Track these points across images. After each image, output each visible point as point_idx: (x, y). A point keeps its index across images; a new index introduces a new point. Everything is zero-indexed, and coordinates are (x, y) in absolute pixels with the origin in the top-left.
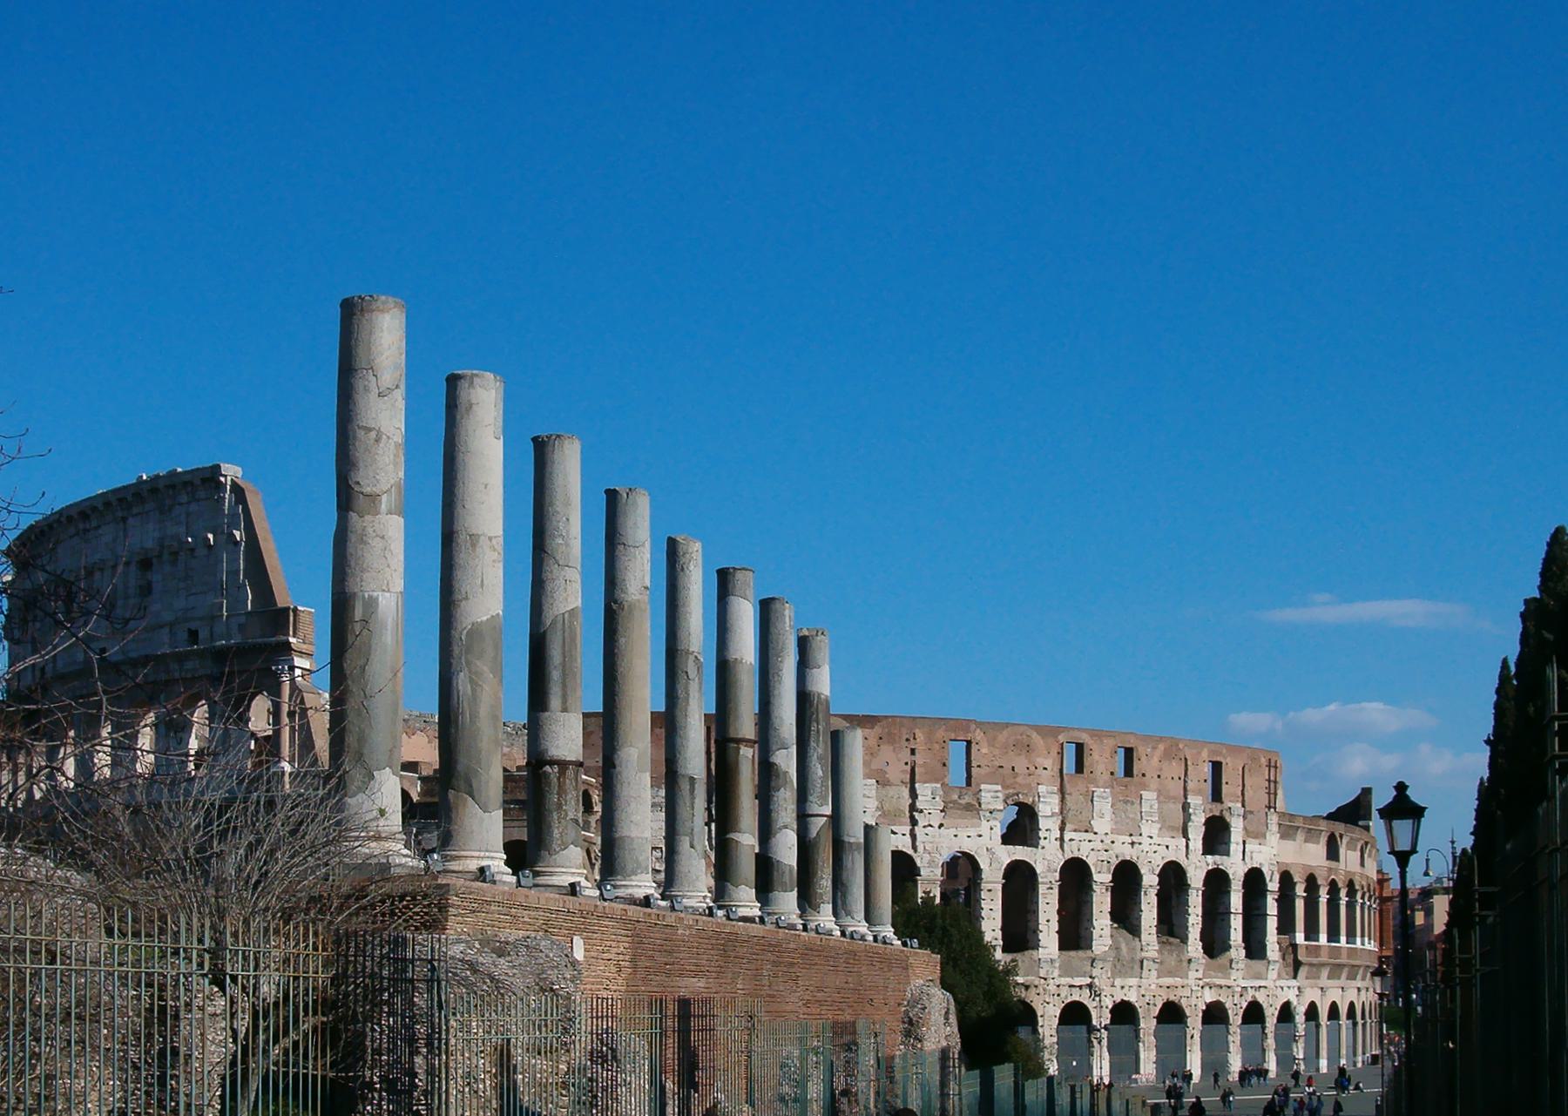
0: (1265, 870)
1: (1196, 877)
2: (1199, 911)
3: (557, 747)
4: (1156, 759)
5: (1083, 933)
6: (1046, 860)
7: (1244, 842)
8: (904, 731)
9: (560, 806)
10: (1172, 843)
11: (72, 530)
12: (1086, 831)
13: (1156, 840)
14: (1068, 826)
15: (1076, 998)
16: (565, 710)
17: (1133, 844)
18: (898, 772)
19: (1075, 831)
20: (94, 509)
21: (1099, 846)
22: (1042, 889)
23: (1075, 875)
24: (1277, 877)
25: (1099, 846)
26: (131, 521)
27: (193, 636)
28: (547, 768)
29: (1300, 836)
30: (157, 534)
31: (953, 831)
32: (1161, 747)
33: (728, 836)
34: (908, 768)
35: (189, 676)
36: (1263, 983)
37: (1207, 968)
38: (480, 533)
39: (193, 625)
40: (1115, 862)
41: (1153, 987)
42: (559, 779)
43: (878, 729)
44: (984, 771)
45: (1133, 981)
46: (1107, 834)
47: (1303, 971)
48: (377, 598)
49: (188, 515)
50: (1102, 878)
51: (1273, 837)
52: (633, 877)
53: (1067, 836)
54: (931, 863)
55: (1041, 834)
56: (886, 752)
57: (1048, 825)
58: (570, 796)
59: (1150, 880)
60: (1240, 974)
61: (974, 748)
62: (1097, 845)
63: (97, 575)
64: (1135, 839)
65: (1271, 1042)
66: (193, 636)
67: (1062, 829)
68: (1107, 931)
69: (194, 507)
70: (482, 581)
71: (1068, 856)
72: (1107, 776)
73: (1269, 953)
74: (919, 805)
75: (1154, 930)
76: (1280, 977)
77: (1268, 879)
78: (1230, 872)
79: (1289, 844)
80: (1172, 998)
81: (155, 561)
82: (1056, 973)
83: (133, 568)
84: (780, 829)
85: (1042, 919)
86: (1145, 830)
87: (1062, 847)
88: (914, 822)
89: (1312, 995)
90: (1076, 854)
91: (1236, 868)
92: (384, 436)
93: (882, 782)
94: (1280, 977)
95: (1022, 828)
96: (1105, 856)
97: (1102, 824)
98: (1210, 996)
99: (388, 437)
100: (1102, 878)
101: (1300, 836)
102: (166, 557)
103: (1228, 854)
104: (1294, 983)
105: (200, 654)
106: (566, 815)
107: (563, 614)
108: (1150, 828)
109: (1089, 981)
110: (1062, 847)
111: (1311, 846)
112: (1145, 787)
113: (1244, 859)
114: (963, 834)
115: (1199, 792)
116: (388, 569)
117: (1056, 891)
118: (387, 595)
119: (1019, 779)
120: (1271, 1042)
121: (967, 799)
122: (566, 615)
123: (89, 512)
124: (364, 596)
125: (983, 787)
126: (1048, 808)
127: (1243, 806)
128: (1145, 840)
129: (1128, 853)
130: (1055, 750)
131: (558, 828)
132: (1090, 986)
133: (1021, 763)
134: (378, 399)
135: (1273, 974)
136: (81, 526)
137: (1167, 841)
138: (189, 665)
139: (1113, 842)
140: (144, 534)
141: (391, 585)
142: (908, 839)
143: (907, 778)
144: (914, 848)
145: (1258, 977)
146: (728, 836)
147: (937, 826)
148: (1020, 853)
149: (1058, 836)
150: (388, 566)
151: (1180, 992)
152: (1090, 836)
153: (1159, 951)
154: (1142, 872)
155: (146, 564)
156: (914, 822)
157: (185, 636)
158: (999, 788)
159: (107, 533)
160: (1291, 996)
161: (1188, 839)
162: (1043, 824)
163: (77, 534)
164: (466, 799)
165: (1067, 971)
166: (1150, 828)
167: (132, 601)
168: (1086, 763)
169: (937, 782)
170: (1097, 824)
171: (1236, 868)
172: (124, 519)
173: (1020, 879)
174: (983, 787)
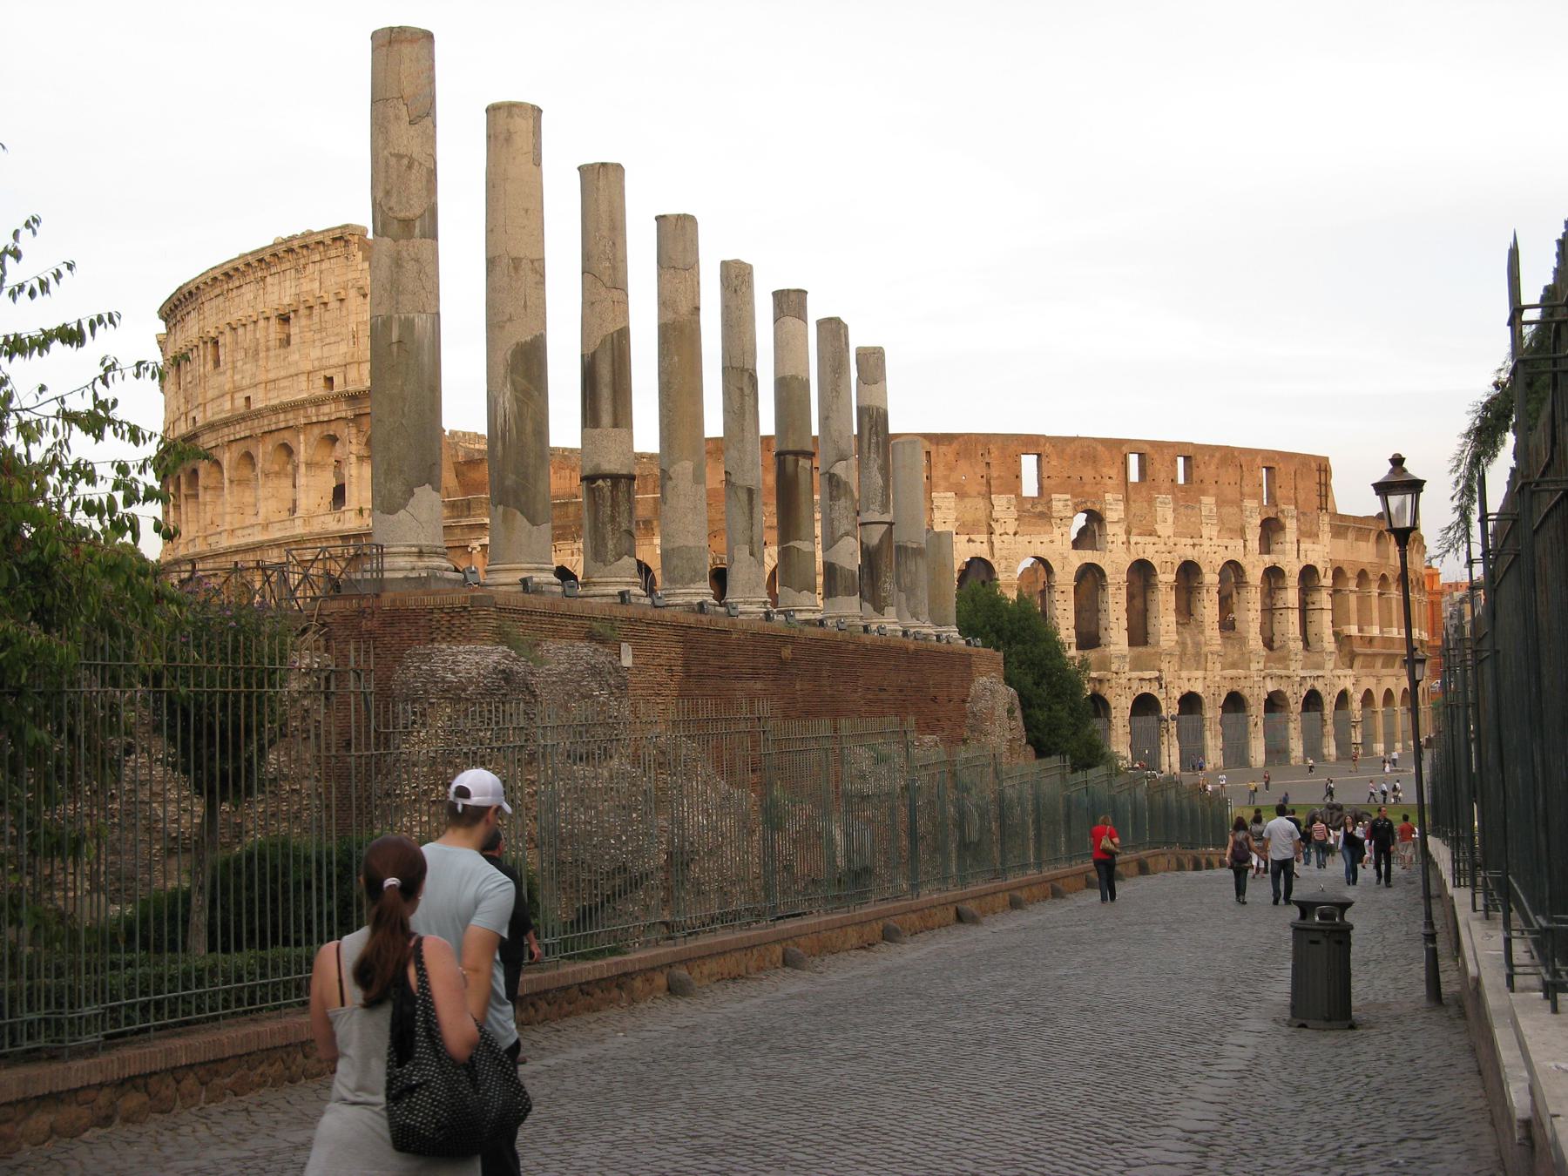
0: (1320, 567)
1: (1254, 575)
2: (1259, 606)
3: (609, 462)
4: (1213, 467)
5: (1151, 629)
6: (1115, 560)
7: (1298, 541)
8: (979, 447)
9: (613, 519)
10: (1231, 544)
11: (218, 291)
12: (1150, 535)
13: (1219, 542)
14: (1134, 531)
15: (1146, 690)
16: (616, 425)
17: (1194, 545)
18: (976, 487)
19: (1140, 535)
20: (237, 269)
21: (1164, 548)
22: (1111, 590)
23: (1142, 572)
24: (1330, 573)
25: (1164, 548)
26: (269, 279)
27: (329, 380)
28: (600, 482)
29: (1351, 535)
30: (293, 290)
31: (1028, 538)
32: (1218, 455)
33: (791, 544)
34: (984, 480)
35: (326, 419)
36: (1320, 673)
37: (1268, 660)
38: (522, 256)
39: (328, 373)
40: (1178, 563)
41: (1217, 679)
42: (612, 492)
43: (955, 445)
44: (1052, 482)
45: (1200, 674)
46: (1169, 537)
47: (1357, 663)
48: (413, 320)
49: (321, 272)
50: (1166, 576)
51: (1325, 536)
52: (692, 586)
53: (1133, 539)
55: (1109, 539)
56: (963, 465)
57: (1114, 532)
58: (622, 508)
59: (1211, 578)
60: (1299, 665)
61: (1043, 458)
62: (1161, 547)
63: (241, 331)
64: (1196, 541)
65: (1329, 728)
66: (329, 380)
67: (1128, 532)
68: (1173, 627)
69: (325, 265)
70: (525, 302)
71: (1135, 557)
72: (1168, 484)
73: (1326, 645)
74: (994, 515)
75: (1216, 626)
76: (1336, 667)
77: (1322, 576)
78: (1286, 570)
79: (1341, 543)
80: (1236, 688)
81: (292, 315)
82: (1127, 668)
83: (273, 321)
84: (842, 536)
85: (1112, 618)
86: (1205, 532)
87: (1128, 549)
89: (1368, 683)
90: (1141, 556)
91: (1292, 568)
92: (416, 164)
93: (961, 494)
94: (1336, 667)
96: (1169, 557)
97: (1165, 528)
98: (1271, 686)
99: (420, 164)
100: (1166, 576)
101: (1351, 535)
102: (302, 311)
103: (1283, 552)
104: (1350, 672)
105: (336, 399)
106: (620, 526)
107: (612, 334)
108: (1209, 531)
109: (1156, 674)
110: (1128, 549)
111: (1362, 544)
112: (1204, 493)
113: (1298, 557)
114: (1036, 540)
115: (1256, 496)
116: (422, 291)
117: (1124, 591)
118: (424, 316)
119: (1087, 488)
120: (1329, 728)
121: (1039, 509)
122: (615, 335)
123: (231, 273)
124: (400, 318)
125: (1053, 496)
126: (1114, 512)
127: (1296, 507)
128: (1206, 542)
129: (1190, 554)
130: (1119, 460)
131: (612, 539)
132: (1159, 679)
133: (1088, 474)
134: (409, 127)
135: (1330, 665)
136: (225, 287)
137: (1226, 542)
138: (325, 409)
139: (1175, 545)
140: (281, 291)
141: (427, 307)
142: (986, 546)
143: (984, 489)
144: (993, 555)
145: (1320, 666)
146: (791, 544)
147: (1011, 533)
148: (1089, 556)
149: (1125, 539)
150: (424, 288)
151: (1242, 683)
152: (1153, 539)
153: (1224, 645)
154: (1204, 571)
155: (285, 319)
157: (322, 382)
158: (1068, 497)
159: (248, 292)
160: (1347, 684)
161: (1245, 541)
162: (1110, 529)
163: (222, 294)
164: (515, 514)
165: (1137, 665)
166: (1209, 531)
167: (272, 353)
168: (1149, 472)
169: (1011, 493)
170: (1159, 528)
171: (1292, 568)
172: (263, 279)
173: (1090, 577)
174: (1053, 496)
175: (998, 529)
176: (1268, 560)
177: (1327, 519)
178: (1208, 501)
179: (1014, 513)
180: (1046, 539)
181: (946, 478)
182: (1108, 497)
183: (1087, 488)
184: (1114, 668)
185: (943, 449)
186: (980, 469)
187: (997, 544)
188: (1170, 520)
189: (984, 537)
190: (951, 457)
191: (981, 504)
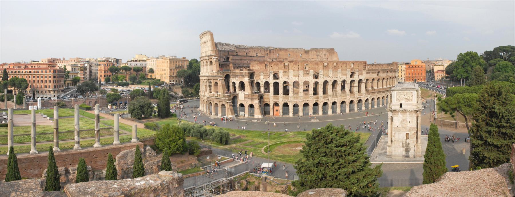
0: (363, 79)
6: (321, 81)
15: (326, 101)
18: (296, 69)
22: (320, 86)
23: (326, 83)
32: (342, 62)
37: (350, 95)
45: (336, 98)
54: (301, 83)
56: (294, 66)
86: (339, 75)
88: (299, 77)
90: (326, 80)
93: (294, 71)
95: (316, 77)
98: (351, 100)
100: (330, 83)
114: (306, 78)
117: (322, 86)
126: (321, 73)
128: (339, 77)
129: (335, 79)
130: (322, 64)
132: (328, 100)
133: (317, 67)
148: (316, 80)
156: (299, 77)
165: (324, 98)
170: (329, 75)
175: (300, 76)
176: (352, 79)
177: (365, 71)
178: (340, 70)
179: (303, 73)
180: (308, 77)
181: (292, 68)
182: (320, 70)
183: (316, 69)
184: (320, 98)
185: (291, 63)
186: (297, 66)
187: (300, 79)
188: (332, 74)
189: (298, 77)
190: (292, 65)
191: (297, 72)
